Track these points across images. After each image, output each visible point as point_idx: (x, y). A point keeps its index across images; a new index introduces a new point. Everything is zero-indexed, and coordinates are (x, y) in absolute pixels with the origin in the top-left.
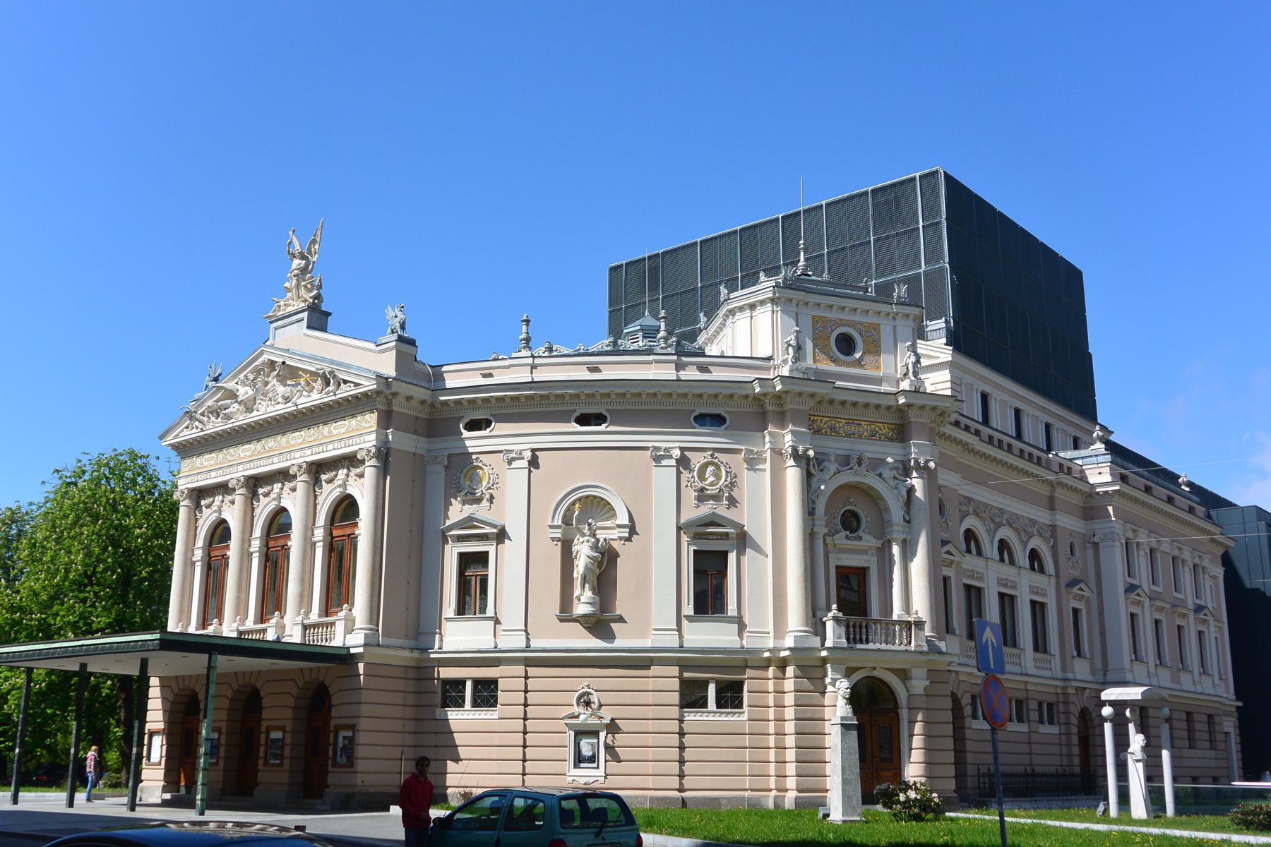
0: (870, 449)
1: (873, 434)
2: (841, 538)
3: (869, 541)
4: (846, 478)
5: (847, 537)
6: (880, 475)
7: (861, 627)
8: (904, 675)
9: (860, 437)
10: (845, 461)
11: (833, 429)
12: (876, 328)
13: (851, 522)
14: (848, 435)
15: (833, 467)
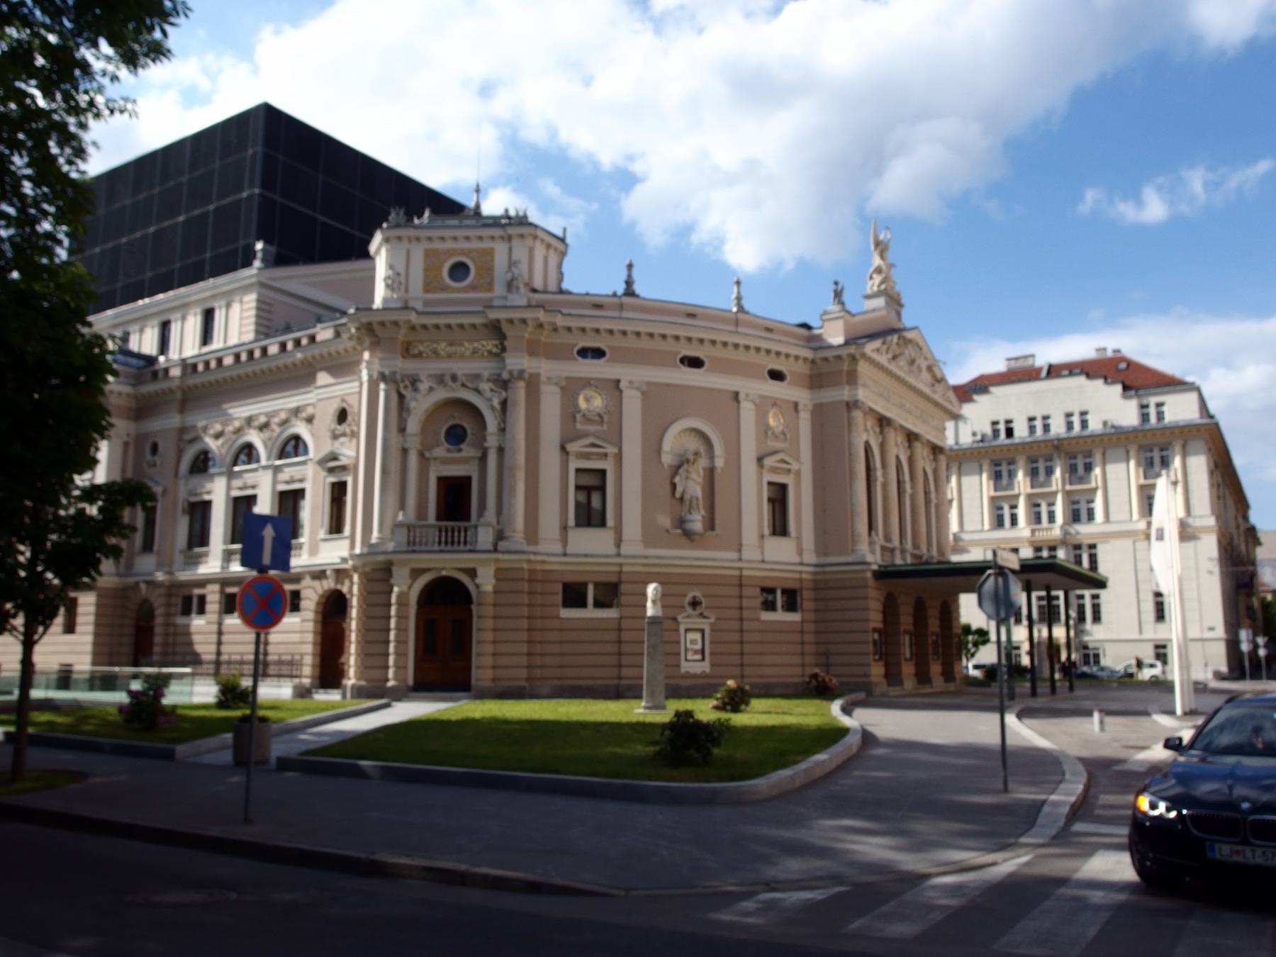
0: (463, 368)
1: (475, 352)
2: (441, 451)
3: (468, 451)
4: (441, 394)
5: (449, 451)
6: (477, 391)
7: (453, 531)
8: (472, 573)
9: (462, 356)
10: (440, 379)
11: (436, 353)
12: (490, 253)
13: (456, 436)
14: (450, 356)
15: (424, 386)
